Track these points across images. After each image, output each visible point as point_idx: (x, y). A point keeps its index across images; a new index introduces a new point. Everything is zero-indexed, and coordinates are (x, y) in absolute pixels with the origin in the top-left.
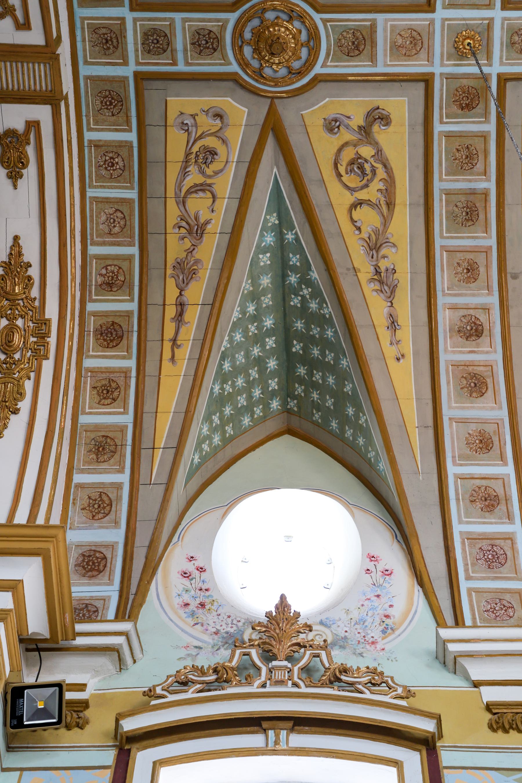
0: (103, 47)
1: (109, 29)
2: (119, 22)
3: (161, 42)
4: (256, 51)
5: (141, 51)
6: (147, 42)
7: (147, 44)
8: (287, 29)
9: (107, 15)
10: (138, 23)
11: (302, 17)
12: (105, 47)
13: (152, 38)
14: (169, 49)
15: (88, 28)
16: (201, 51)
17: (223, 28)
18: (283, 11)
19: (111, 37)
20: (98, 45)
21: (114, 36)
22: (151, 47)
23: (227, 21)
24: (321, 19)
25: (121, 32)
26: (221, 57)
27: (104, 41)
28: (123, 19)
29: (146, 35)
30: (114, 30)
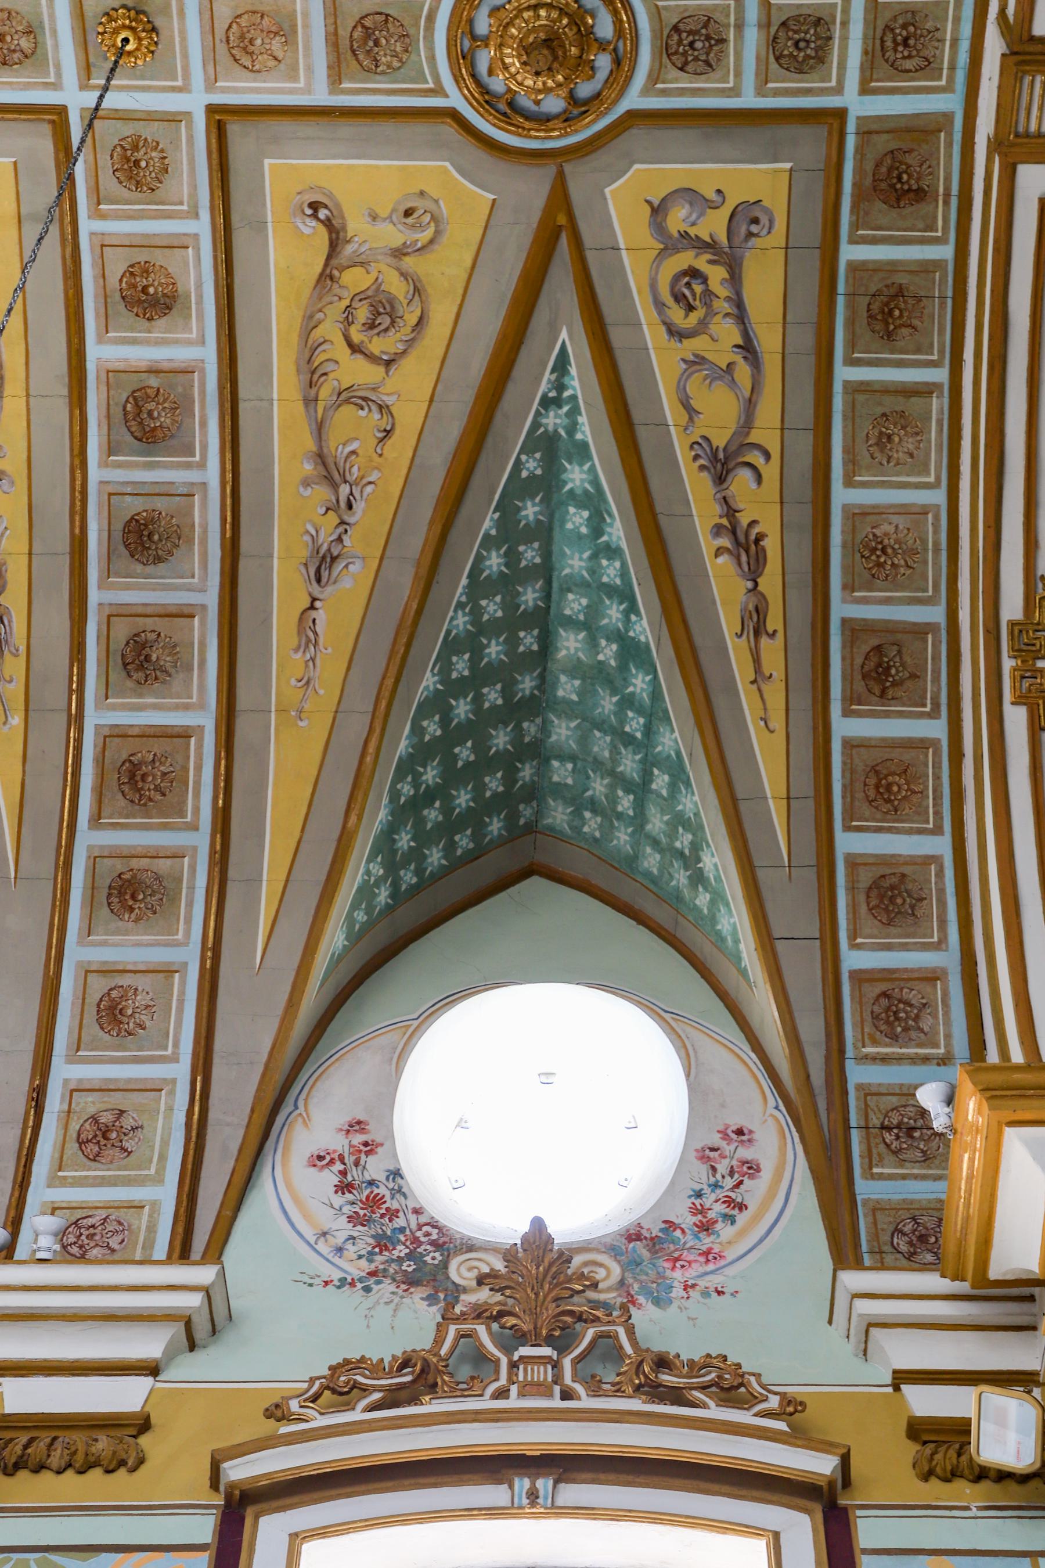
0: (916, 28)
1: (896, 69)
2: (873, 84)
3: (789, 43)
4: (586, 37)
5: (834, 22)
6: (819, 43)
7: (821, 38)
8: (521, 84)
9: (897, 98)
10: (833, 83)
11: (487, 102)
12: (912, 29)
13: (809, 51)
14: (773, 30)
15: (942, 69)
16: (706, 26)
17: (654, 77)
18: (528, 116)
19: (895, 51)
20: (925, 33)
21: (888, 54)
22: (812, 31)
23: (646, 91)
24: (447, 96)
25: (872, 62)
26: (664, 13)
27: (911, 42)
28: (865, 90)
29: (820, 58)
30: (886, 66)
